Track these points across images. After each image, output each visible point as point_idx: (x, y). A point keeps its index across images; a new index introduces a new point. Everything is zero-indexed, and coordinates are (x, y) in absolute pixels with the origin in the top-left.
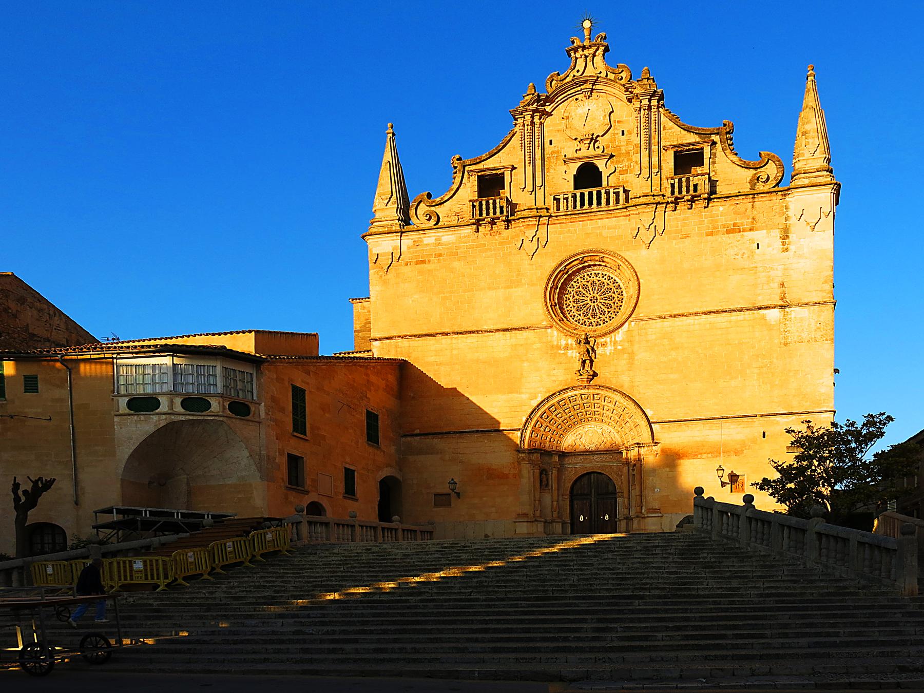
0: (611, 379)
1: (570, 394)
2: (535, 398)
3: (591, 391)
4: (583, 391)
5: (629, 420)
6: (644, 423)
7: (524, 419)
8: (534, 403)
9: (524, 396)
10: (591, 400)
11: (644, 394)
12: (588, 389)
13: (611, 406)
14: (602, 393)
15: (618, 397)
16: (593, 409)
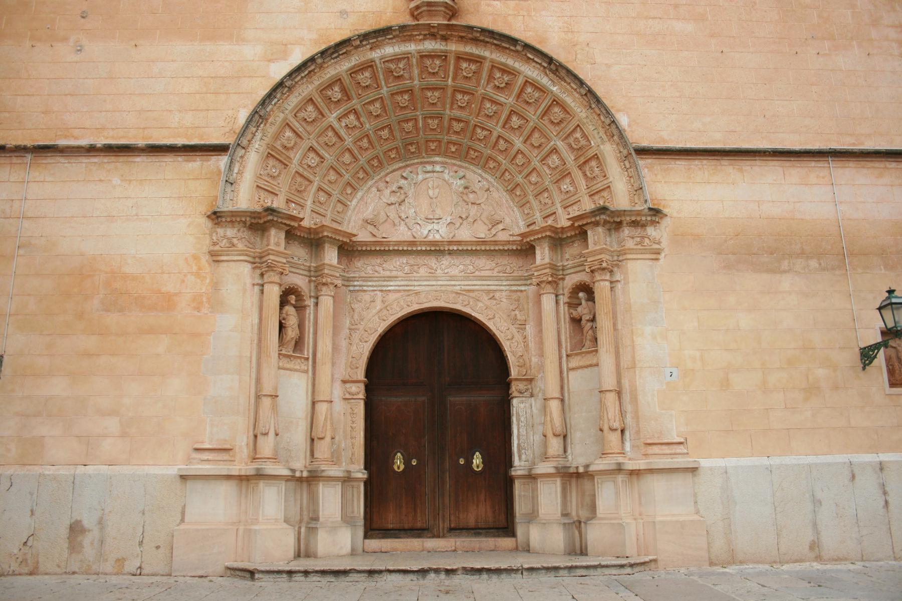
0: (510, 19)
1: (389, 50)
2: (284, 55)
3: (453, 47)
4: (430, 45)
5: (560, 145)
6: (609, 151)
7: (243, 116)
8: (279, 70)
9: (250, 52)
10: (446, 78)
11: (609, 66)
12: (445, 38)
13: (508, 100)
14: (486, 53)
15: (530, 71)
16: (448, 112)
